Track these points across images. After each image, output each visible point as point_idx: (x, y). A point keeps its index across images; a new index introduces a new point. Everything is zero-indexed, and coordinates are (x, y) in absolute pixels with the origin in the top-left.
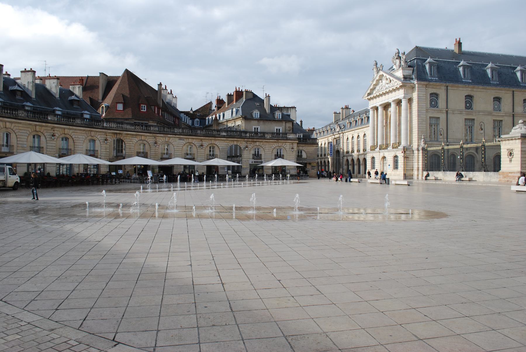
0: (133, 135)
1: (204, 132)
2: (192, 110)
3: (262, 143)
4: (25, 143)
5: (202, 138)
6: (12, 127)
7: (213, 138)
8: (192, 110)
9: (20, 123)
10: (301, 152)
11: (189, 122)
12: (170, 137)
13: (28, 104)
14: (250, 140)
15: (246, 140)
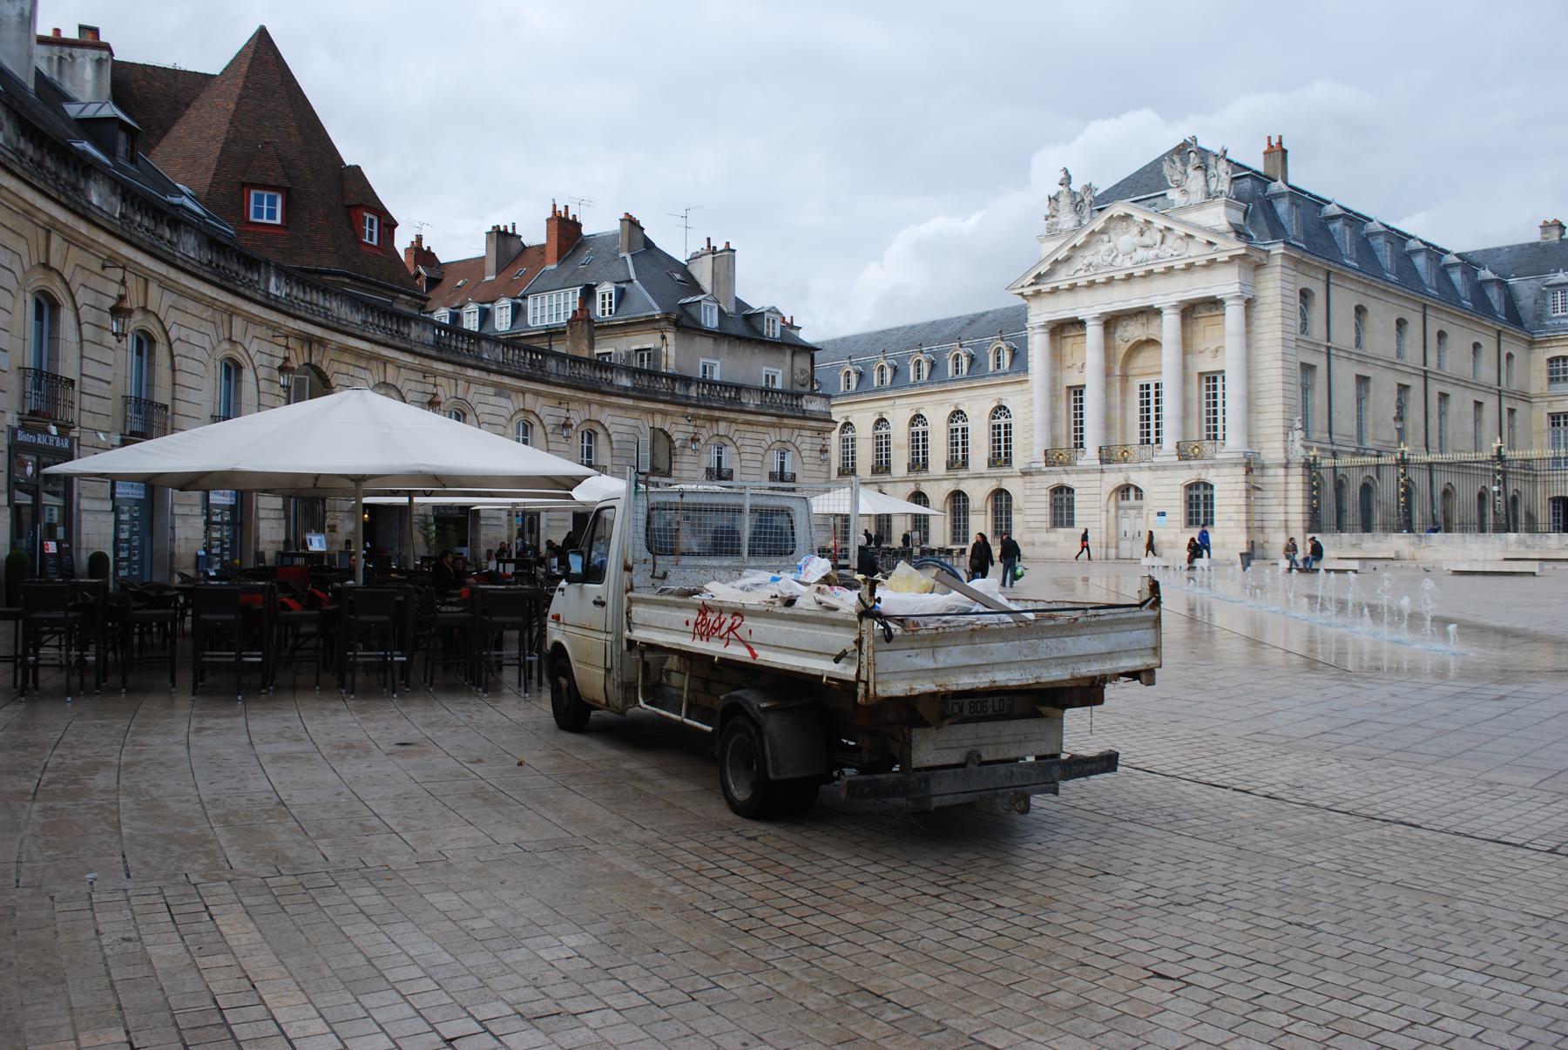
0: (358, 353)
3: (734, 427)
5: (565, 392)
7: (597, 397)
12: (469, 381)
14: (703, 412)
15: (690, 410)
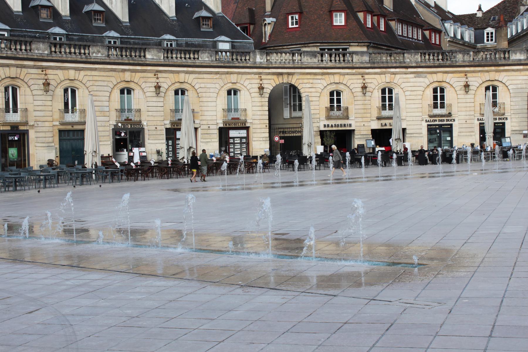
0: (315, 74)
1: (470, 57)
2: (480, 9)
4: (107, 104)
6: (80, 78)
7: (493, 68)
8: (480, 9)
9: (95, 69)
11: (468, 35)
13: (113, 34)
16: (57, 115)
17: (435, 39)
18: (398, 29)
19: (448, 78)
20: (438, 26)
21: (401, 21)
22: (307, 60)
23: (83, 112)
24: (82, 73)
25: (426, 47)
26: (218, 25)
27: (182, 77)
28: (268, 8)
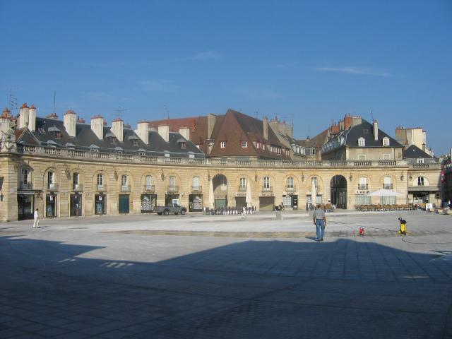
2: (308, 138)
8: (308, 138)
10: (422, 179)
16: (119, 188)
17: (287, 153)
18: (271, 149)
19: (295, 173)
20: (289, 146)
21: (272, 145)
22: (229, 164)
23: (130, 186)
24: (130, 168)
25: (284, 158)
26: (189, 146)
27: (173, 171)
28: (209, 137)
